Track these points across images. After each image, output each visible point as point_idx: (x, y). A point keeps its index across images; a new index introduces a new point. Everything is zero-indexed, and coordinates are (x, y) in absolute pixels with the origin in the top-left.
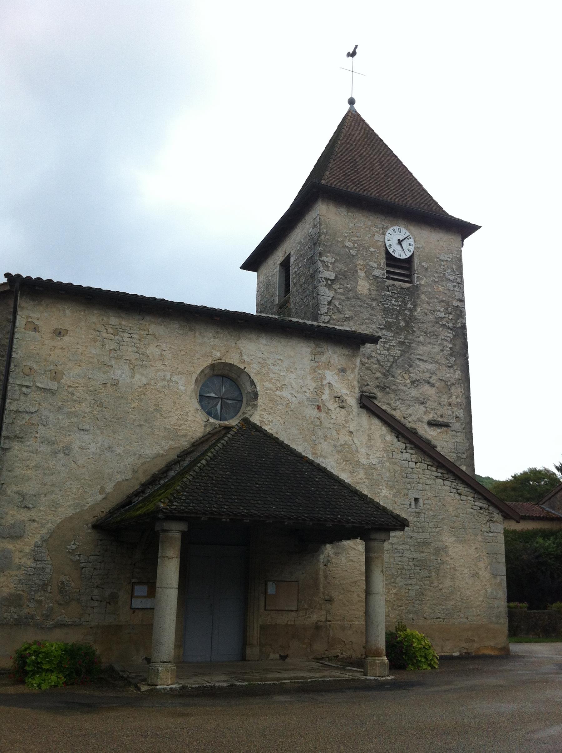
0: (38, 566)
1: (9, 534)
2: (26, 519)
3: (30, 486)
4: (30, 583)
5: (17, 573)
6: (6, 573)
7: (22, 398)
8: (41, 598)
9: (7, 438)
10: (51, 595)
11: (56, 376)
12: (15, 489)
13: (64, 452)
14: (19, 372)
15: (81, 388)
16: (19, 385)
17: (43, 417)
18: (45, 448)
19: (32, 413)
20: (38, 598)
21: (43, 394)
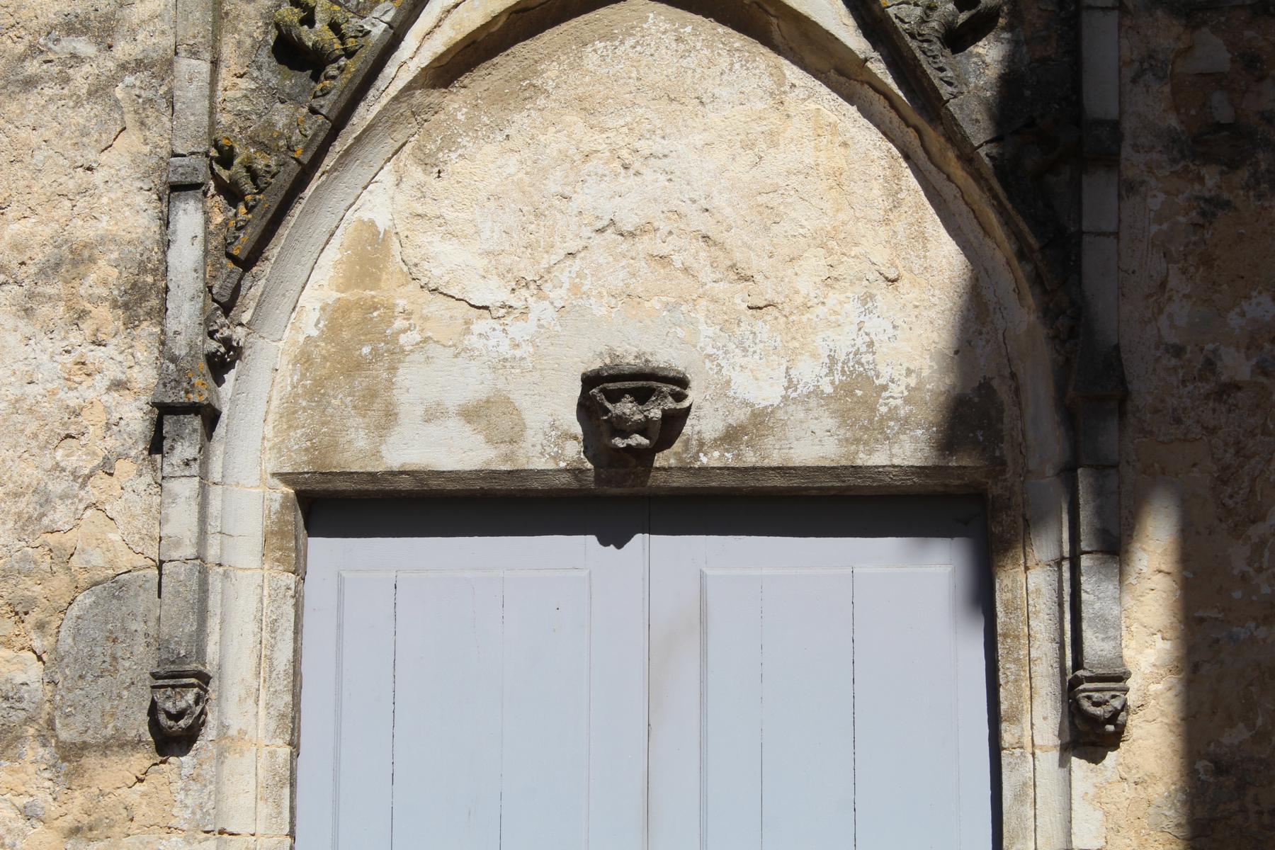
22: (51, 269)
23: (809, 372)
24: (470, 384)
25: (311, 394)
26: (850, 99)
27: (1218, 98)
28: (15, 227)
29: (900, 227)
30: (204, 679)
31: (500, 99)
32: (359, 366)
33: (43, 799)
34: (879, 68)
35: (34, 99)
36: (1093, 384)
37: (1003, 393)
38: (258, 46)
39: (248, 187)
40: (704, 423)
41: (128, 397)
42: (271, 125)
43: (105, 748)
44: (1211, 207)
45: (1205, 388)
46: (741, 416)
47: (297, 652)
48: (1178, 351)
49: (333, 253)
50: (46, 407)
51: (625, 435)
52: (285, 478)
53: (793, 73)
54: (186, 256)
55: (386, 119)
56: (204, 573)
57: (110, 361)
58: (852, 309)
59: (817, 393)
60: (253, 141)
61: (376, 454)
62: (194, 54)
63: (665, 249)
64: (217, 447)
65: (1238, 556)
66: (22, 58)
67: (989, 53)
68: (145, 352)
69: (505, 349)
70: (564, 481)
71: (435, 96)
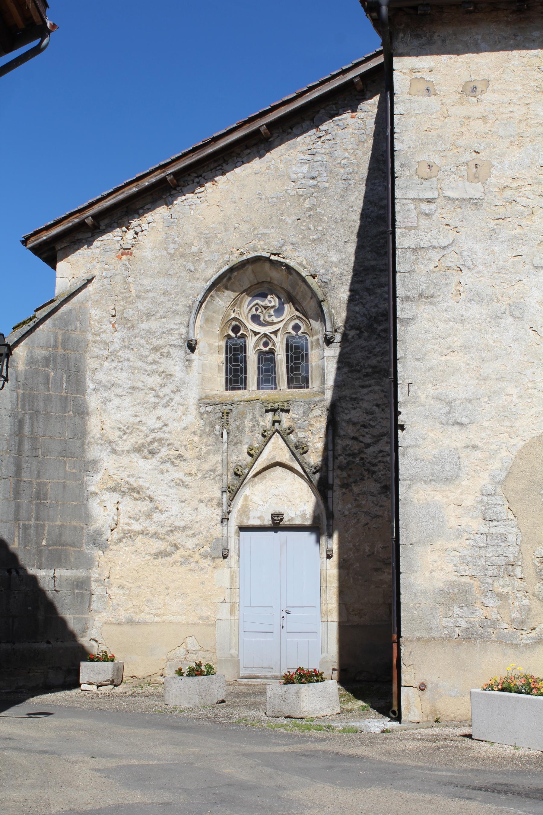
0: (493, 530)
1: (432, 474)
2: (459, 445)
3: (459, 384)
4: (482, 562)
5: (456, 545)
6: (438, 544)
7: (423, 222)
8: (506, 590)
9: (407, 299)
10: (523, 584)
11: (477, 171)
12: (432, 391)
13: (512, 315)
14: (411, 176)
15: (529, 188)
16: (413, 199)
17: (464, 253)
18: (476, 311)
19: (444, 248)
20: (500, 590)
21: (459, 210)
22: (209, 501)
23: (298, 513)
24: (258, 514)
27: (345, 480)
32: (245, 512)
34: (306, 476)
35: (206, 480)
36: (330, 515)
37: (321, 515)
40: (286, 519)
43: (217, 558)
44: (344, 494)
46: (290, 518)
48: (340, 511)
49: (242, 498)
53: (296, 476)
54: (225, 500)
55: (248, 482)
57: (216, 512)
58: (303, 505)
60: (232, 485)
64: (229, 522)
65: (346, 535)
67: (318, 474)
68: (220, 511)
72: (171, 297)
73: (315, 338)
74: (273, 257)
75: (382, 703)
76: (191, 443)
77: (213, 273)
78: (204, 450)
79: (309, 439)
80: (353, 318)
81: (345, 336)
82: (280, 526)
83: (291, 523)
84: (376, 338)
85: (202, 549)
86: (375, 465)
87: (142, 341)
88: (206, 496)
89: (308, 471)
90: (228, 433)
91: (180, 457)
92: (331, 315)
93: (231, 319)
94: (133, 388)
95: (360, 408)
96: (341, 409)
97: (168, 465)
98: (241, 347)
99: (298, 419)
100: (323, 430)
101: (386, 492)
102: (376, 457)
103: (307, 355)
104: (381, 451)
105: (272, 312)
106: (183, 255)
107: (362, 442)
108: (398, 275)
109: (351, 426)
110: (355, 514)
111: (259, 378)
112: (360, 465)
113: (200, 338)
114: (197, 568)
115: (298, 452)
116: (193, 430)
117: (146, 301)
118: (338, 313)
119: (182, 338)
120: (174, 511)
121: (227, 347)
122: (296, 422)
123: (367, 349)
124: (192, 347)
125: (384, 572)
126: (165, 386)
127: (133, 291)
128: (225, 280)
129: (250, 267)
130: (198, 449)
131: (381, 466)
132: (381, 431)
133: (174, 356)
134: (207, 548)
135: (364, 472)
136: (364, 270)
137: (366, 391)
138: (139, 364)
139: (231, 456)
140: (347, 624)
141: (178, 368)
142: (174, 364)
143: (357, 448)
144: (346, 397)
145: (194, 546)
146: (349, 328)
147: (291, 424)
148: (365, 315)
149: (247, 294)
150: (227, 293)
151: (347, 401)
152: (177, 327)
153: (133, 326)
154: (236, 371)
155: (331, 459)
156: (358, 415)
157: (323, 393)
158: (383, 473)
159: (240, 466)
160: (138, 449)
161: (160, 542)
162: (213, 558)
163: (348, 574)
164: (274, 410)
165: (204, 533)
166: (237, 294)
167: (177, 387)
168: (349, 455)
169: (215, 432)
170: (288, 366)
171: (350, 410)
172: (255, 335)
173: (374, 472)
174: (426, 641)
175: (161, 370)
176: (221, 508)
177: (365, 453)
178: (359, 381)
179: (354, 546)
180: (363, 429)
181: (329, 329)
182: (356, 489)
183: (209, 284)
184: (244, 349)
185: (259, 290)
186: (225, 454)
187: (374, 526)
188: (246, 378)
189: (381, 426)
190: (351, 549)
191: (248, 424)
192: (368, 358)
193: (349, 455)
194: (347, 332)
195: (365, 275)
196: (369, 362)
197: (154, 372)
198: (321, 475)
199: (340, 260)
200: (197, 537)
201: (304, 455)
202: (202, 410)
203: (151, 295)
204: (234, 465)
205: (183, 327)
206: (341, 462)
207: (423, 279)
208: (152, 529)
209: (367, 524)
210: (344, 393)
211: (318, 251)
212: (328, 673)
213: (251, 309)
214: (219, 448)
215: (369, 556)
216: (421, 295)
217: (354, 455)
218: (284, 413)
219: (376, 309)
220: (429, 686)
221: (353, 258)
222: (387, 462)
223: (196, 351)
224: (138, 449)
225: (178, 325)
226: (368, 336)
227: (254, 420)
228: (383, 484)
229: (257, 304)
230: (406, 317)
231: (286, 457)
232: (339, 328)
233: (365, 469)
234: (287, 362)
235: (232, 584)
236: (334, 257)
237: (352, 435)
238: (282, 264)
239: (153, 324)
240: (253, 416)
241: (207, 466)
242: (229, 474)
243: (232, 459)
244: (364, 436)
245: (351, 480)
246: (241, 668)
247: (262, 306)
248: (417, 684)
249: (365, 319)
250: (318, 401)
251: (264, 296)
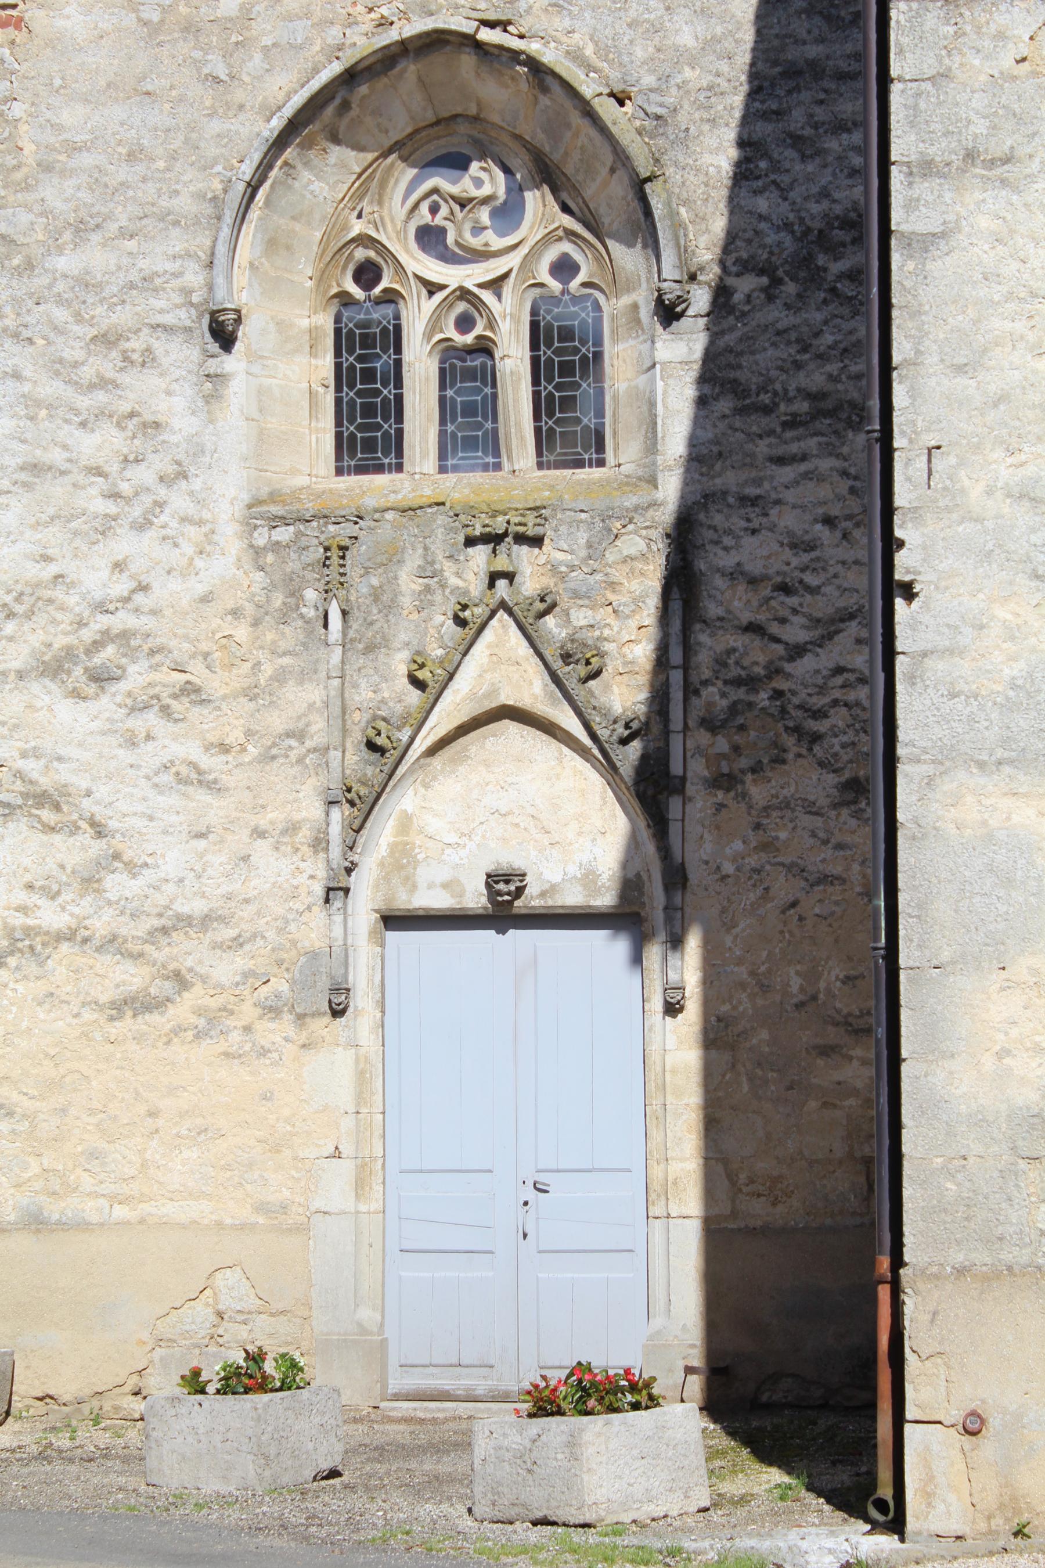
1: (1005, 742)
6: (1021, 968)
9: (927, 168)
12: (1003, 470)
22: (284, 832)
23: (573, 870)
24: (444, 874)
25: (384, 878)
26: (587, 761)
27: (724, 763)
28: (270, 816)
29: (606, 812)
30: (348, 990)
31: (454, 761)
32: (402, 867)
33: (292, 1034)
34: (596, 752)
35: (275, 765)
36: (676, 877)
37: (645, 877)
38: (359, 742)
39: (357, 801)
40: (533, 889)
41: (315, 882)
42: (365, 775)
44: (720, 807)
45: (717, 877)
46: (547, 886)
47: (383, 977)
48: (707, 863)
49: (391, 823)
50: (285, 885)
51: (501, 895)
52: (376, 911)
53: (565, 750)
54: (335, 829)
55: (410, 770)
56: (346, 950)
57: (308, 867)
59: (575, 877)
60: (359, 781)
61: (410, 902)
62: (335, 749)
63: (517, 821)
64: (350, 901)
65: (728, 940)
66: (270, 748)
67: (636, 745)
69: (457, 860)
70: (481, 911)
71: (428, 760)
72: (154, 167)
73: (625, 300)
74: (486, 35)
75: (843, 1477)
76: (224, 647)
77: (290, 89)
78: (268, 670)
79: (606, 632)
80: (750, 234)
81: (721, 294)
82: (515, 911)
83: (550, 903)
84: (825, 302)
85: (265, 989)
86: (819, 714)
87: (61, 315)
88: (273, 817)
89: (603, 733)
90: (344, 613)
91: (190, 691)
92: (677, 226)
93: (353, 240)
94: (35, 468)
95: (772, 528)
96: (709, 534)
97: (152, 719)
98: (385, 331)
99: (572, 568)
100: (653, 603)
101: (855, 802)
102: (822, 690)
103: (598, 356)
104: (839, 670)
105: (484, 215)
106: (190, 29)
107: (777, 640)
108: (896, 89)
109: (741, 588)
110: (758, 871)
111: (442, 434)
112: (772, 715)
113: (252, 304)
114: (248, 1047)
115: (571, 674)
116: (230, 605)
117: (73, 182)
118: (699, 218)
119: (192, 304)
120: (173, 864)
121: (338, 332)
122: (563, 578)
123: (793, 336)
124: (223, 334)
125: (850, 1059)
126: (137, 461)
127: (29, 148)
128: (330, 110)
129: (412, 68)
130: (249, 665)
131: (839, 718)
132: (841, 603)
133: (165, 361)
134: (280, 985)
135: (785, 736)
136: (786, 75)
137: (792, 475)
138: (50, 388)
139: (355, 686)
140: (731, 1226)
141: (179, 403)
142: (167, 386)
143: (762, 659)
144: (725, 493)
145: (238, 978)
146: (734, 269)
147: (548, 582)
148: (787, 226)
149: (404, 159)
150: (337, 153)
151: (729, 506)
152: (173, 269)
153: (30, 265)
154: (369, 410)
155: (677, 695)
156: (765, 553)
157: (653, 482)
158: (844, 739)
159: (384, 719)
160: (53, 668)
161: (129, 966)
162: (301, 1017)
163: (733, 1066)
164: (494, 539)
165: (270, 934)
166: (370, 156)
167: (179, 463)
168: (737, 682)
169: (304, 610)
170: (536, 395)
171: (738, 538)
172: (431, 293)
173: (816, 738)
174: (986, 1278)
175: (125, 407)
176: (322, 855)
177: (788, 676)
178: (767, 441)
179: (753, 973)
180: (782, 598)
181: (670, 271)
182: (758, 792)
183: (277, 123)
184: (394, 338)
185: (444, 143)
186: (336, 682)
187: (817, 911)
188: (400, 433)
189: (839, 587)
190: (742, 986)
191: (408, 582)
192: (798, 366)
193: (737, 682)
194: (730, 281)
195: (789, 92)
196: (801, 380)
197: (102, 414)
198: (645, 748)
199: (706, 42)
200: (247, 947)
201: (592, 683)
202: (261, 538)
203: (87, 160)
204: (366, 716)
205: (192, 266)
206: (710, 704)
207: (979, 101)
208: (101, 925)
209: (794, 904)
210: (718, 481)
211: (632, 14)
212: (671, 1382)
213: (416, 206)
214: (317, 661)
215: (799, 1006)
216: (970, 156)
217: (751, 683)
218: (525, 549)
219: (825, 204)
220: (994, 1422)
221: (748, 36)
222: (858, 704)
223: (238, 346)
224: (53, 668)
225: (179, 262)
226: (799, 296)
227: (429, 572)
228: (847, 775)
229: (435, 191)
230: (921, 227)
231: (531, 689)
232: (702, 269)
233: (787, 728)
234: (536, 381)
235: (361, 1097)
236: (686, 35)
237: (746, 617)
238: (515, 55)
239: (94, 258)
240: (425, 556)
241: (277, 722)
242: (349, 745)
243: (357, 698)
244: (783, 621)
245: (744, 763)
246: (390, 1369)
247: (453, 198)
248: (955, 1414)
249: (788, 241)
250: (636, 509)
251: (458, 163)
